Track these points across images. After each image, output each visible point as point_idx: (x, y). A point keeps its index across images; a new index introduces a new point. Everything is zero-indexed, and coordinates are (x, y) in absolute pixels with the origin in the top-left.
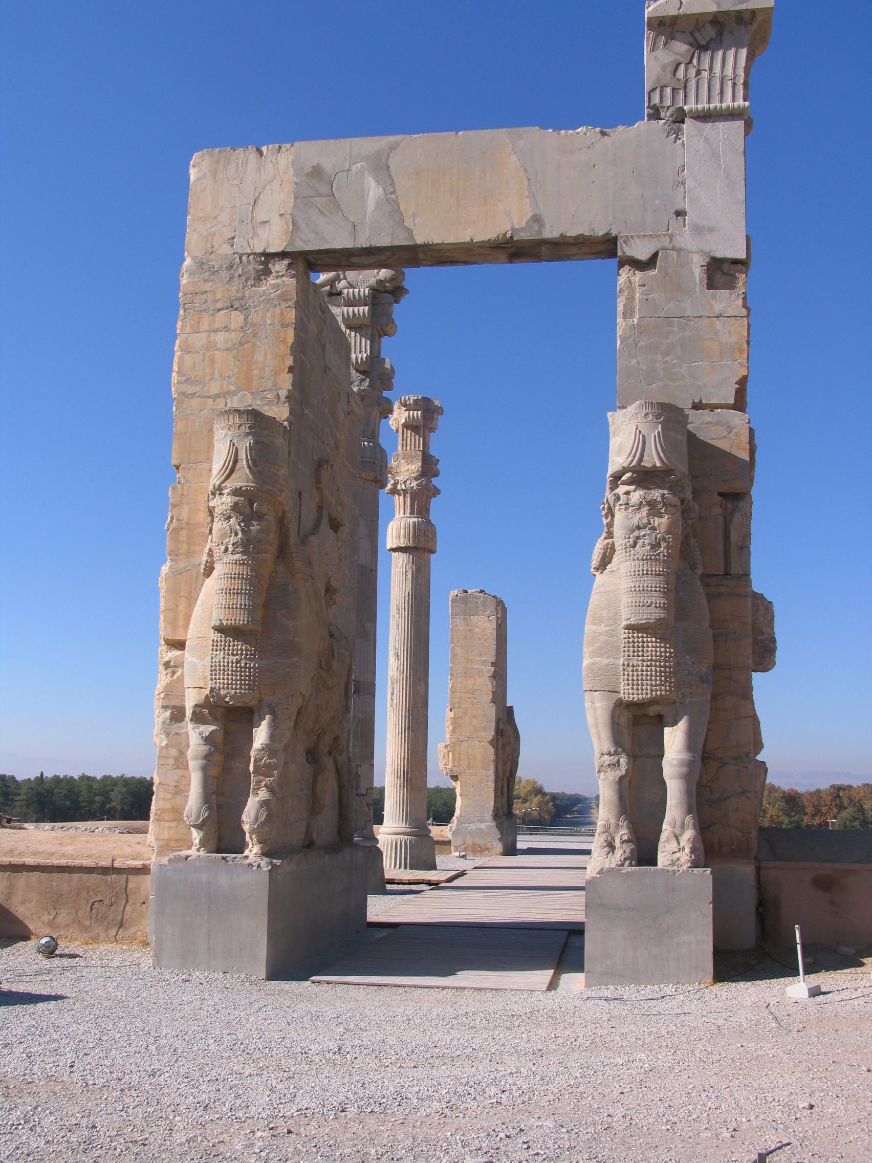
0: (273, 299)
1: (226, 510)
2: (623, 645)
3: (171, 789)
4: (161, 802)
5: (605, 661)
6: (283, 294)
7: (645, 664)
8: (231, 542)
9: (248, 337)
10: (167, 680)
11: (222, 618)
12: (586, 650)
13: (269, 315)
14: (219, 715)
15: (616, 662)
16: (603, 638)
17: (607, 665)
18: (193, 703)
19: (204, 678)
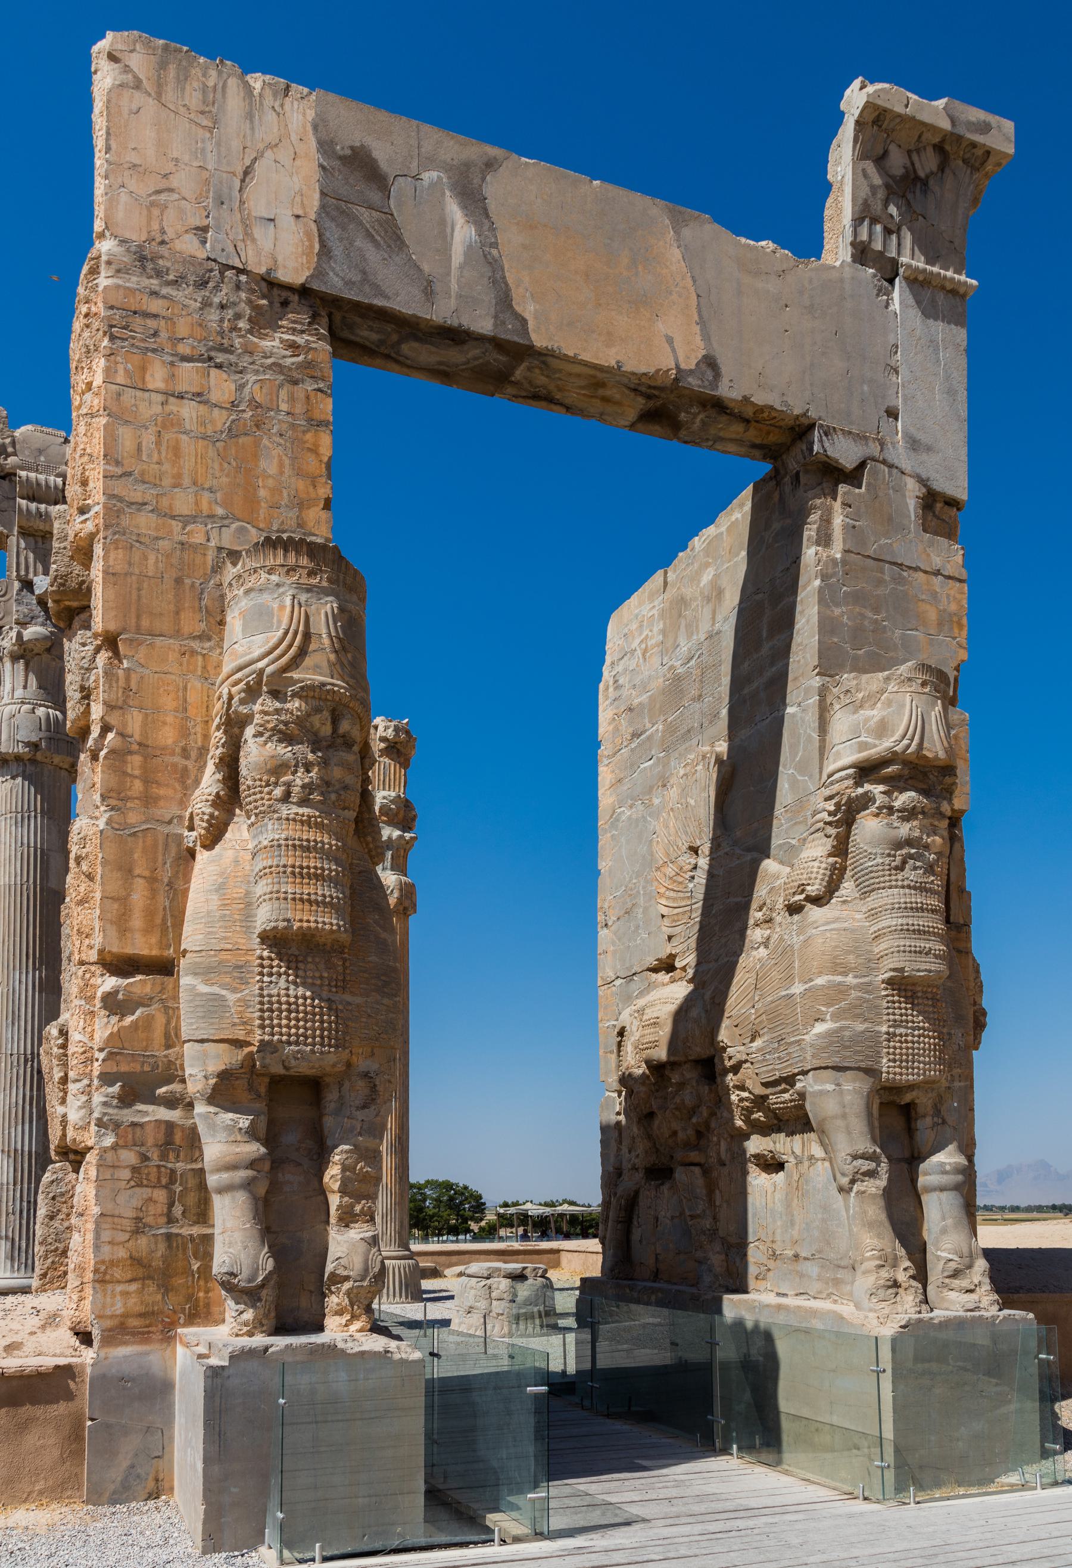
0: (290, 369)
1: (286, 723)
2: (885, 1005)
3: (128, 1225)
4: (106, 1249)
5: (860, 1027)
6: (308, 365)
7: (916, 1032)
8: (299, 782)
9: (245, 425)
10: (110, 1026)
11: (289, 915)
12: (823, 1009)
13: (283, 394)
14: (263, 1090)
15: (877, 1028)
16: (854, 994)
17: (863, 1032)
18: (215, 1066)
19: (245, 1023)
